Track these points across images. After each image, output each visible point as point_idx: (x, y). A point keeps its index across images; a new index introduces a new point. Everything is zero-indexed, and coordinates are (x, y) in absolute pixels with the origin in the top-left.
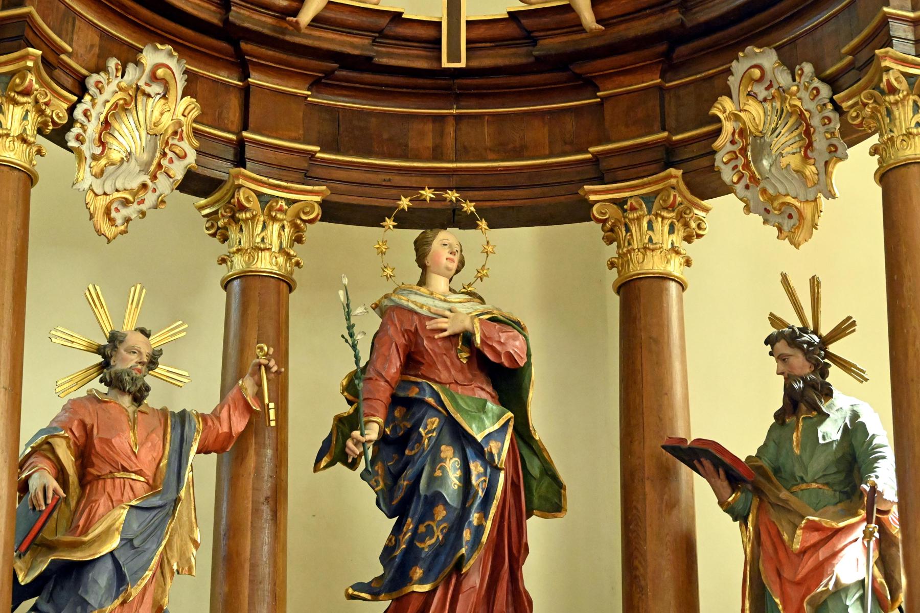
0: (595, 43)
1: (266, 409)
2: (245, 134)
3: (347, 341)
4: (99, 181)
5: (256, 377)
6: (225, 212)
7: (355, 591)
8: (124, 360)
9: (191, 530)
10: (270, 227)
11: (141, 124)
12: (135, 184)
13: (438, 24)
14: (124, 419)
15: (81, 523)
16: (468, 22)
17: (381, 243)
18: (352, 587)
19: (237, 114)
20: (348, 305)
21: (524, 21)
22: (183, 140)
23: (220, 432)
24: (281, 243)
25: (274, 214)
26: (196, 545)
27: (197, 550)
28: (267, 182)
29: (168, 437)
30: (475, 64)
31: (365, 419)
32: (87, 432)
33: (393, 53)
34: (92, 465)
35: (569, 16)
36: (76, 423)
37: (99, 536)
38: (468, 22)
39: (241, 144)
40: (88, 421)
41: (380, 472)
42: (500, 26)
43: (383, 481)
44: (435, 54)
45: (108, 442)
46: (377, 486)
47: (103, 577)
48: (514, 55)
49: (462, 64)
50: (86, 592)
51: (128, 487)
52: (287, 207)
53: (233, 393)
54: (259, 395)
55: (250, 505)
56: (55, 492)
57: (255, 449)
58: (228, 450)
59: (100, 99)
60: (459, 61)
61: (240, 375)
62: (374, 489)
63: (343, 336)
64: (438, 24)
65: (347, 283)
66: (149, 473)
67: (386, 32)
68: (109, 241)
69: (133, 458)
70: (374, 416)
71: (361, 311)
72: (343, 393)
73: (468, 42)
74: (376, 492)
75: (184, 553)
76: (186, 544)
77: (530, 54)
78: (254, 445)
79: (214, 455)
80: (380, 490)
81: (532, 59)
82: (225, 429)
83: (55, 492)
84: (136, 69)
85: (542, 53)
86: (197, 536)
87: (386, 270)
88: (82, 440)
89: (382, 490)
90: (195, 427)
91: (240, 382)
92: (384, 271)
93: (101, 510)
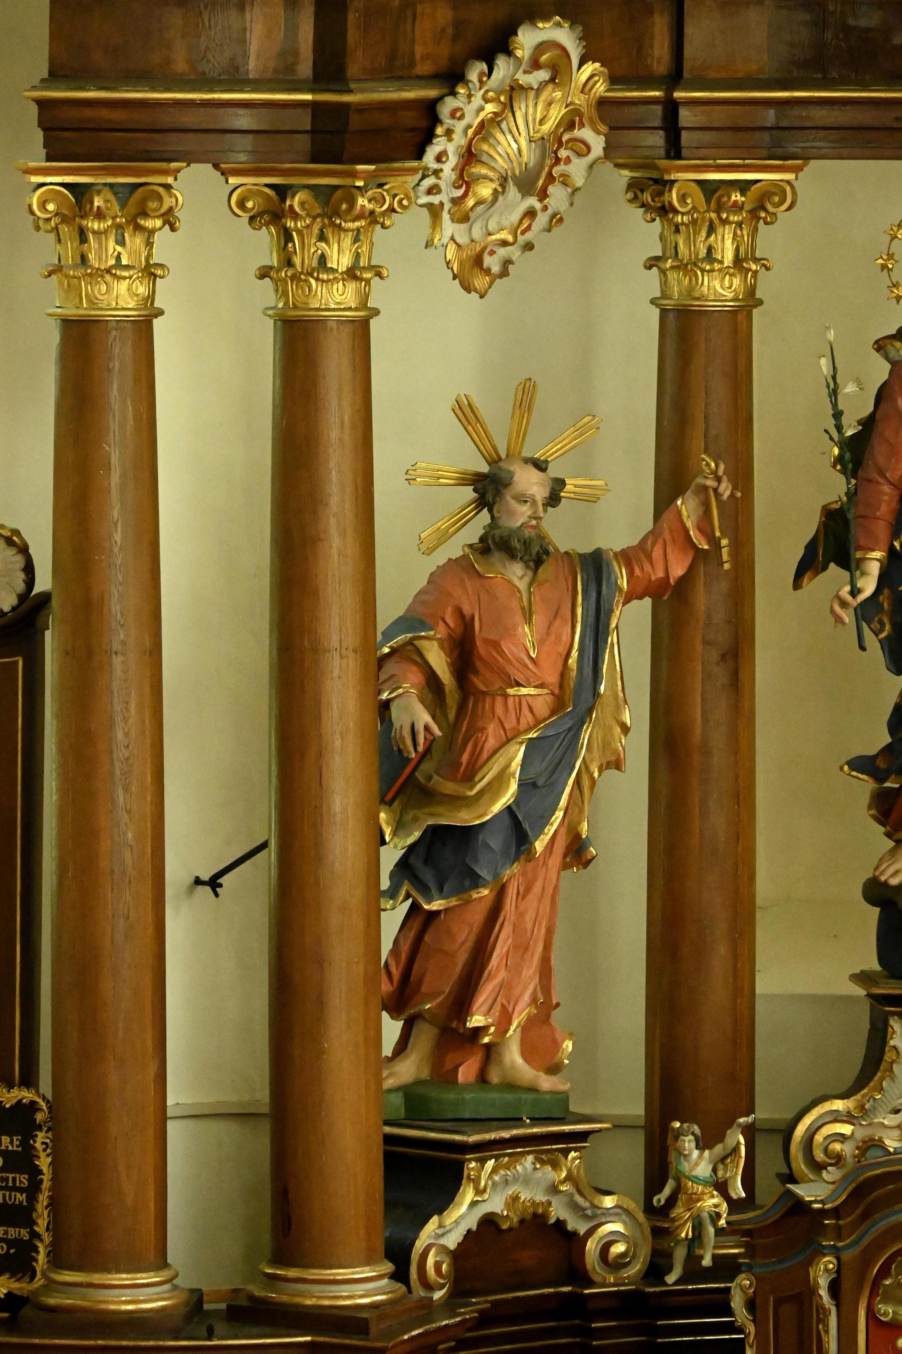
1: (715, 543)
2: (677, 95)
3: (831, 438)
4: (464, 226)
5: (702, 497)
6: (653, 200)
7: (853, 770)
8: (511, 513)
9: (618, 710)
10: (720, 230)
11: (521, 130)
12: (515, 217)
14: (515, 604)
15: (465, 758)
17: (885, 257)
18: (847, 763)
19: (666, 45)
20: (834, 378)
22: (584, 127)
23: (653, 579)
24: (737, 250)
25: (724, 216)
26: (625, 729)
27: (625, 736)
28: (714, 164)
29: (579, 611)
31: (859, 555)
32: (467, 624)
34: (476, 672)
36: (449, 610)
37: (489, 784)
39: (671, 108)
40: (467, 610)
41: (886, 605)
43: (890, 621)
45: (496, 645)
46: (882, 630)
47: (495, 841)
50: (476, 860)
51: (525, 710)
52: (743, 199)
53: (668, 515)
54: (705, 527)
55: (699, 668)
56: (427, 728)
57: (705, 583)
58: (665, 598)
59: (459, 126)
61: (679, 491)
62: (877, 635)
63: (826, 431)
65: (832, 339)
66: (552, 678)
68: (482, 297)
69: (530, 665)
70: (873, 550)
71: (853, 390)
72: (834, 467)
74: (880, 641)
75: (609, 744)
76: (611, 728)
78: (702, 577)
79: (648, 601)
80: (885, 638)
82: (660, 574)
83: (427, 728)
84: (508, 63)
86: (627, 718)
87: (895, 291)
88: (459, 631)
89: (888, 638)
90: (617, 582)
91: (679, 503)
92: (892, 292)
93: (491, 743)
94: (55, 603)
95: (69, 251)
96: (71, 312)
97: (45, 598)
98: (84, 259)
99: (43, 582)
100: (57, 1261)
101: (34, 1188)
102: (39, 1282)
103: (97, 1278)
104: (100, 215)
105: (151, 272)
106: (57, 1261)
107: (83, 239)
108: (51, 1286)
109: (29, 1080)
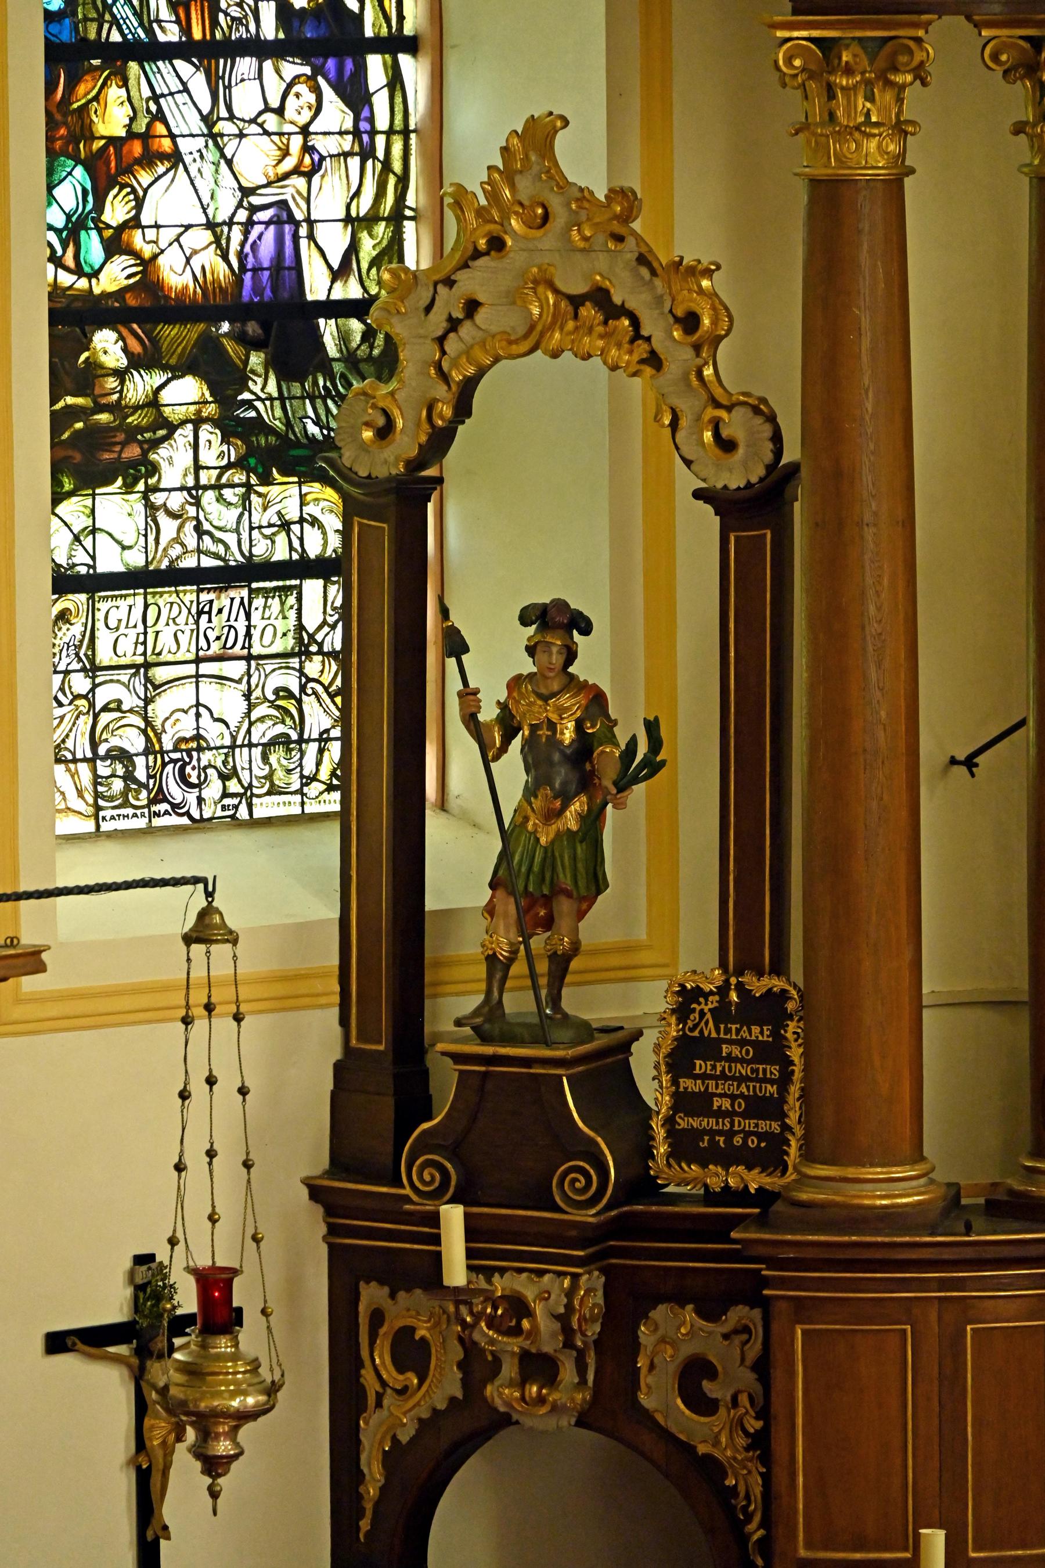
94: (804, 473)
95: (817, 108)
96: (820, 172)
97: (794, 469)
98: (832, 116)
99: (791, 453)
100: (809, 1155)
101: (785, 1080)
102: (791, 1176)
103: (851, 1172)
104: (848, 71)
105: (901, 129)
106: (809, 1155)
107: (831, 96)
108: (804, 1180)
109: (779, 968)
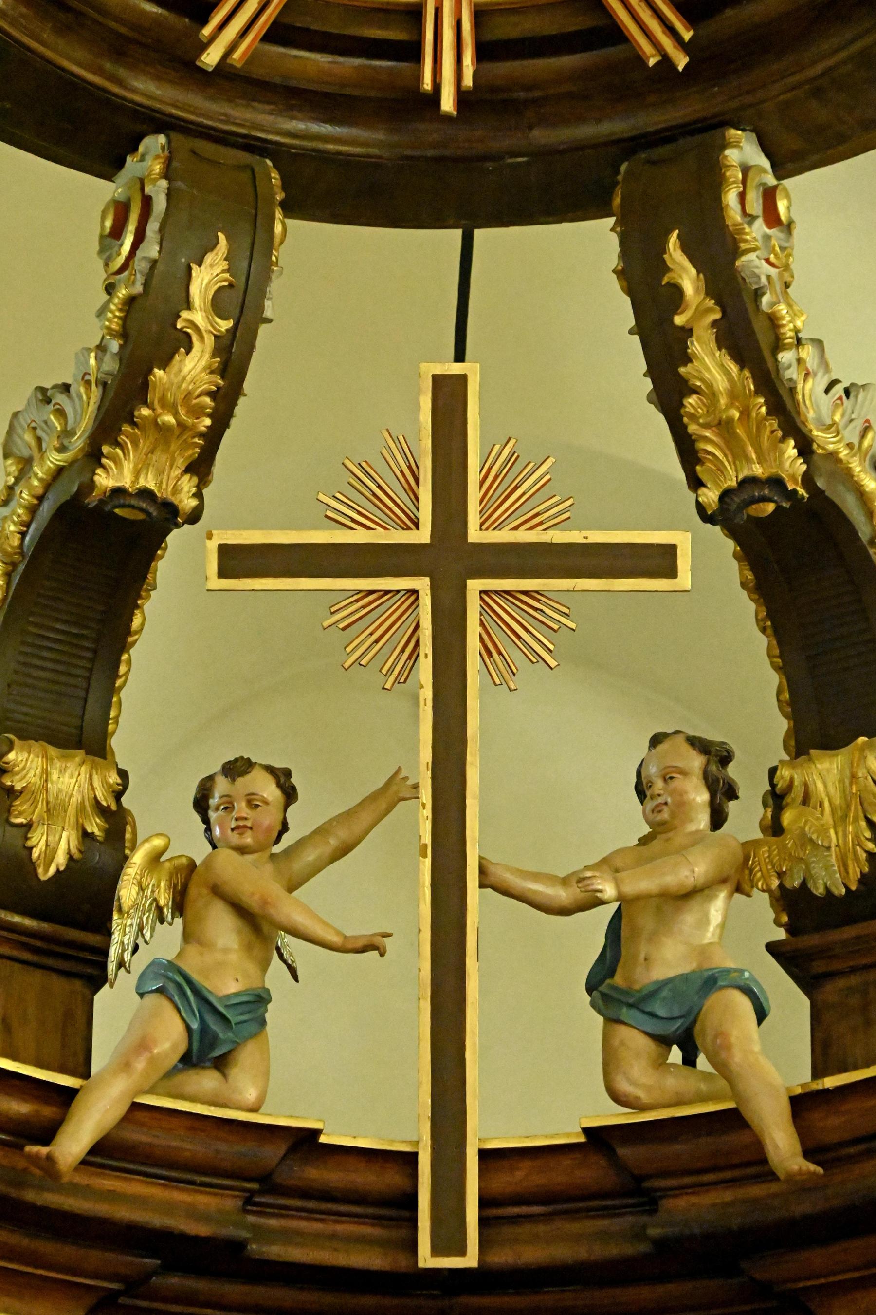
0: (803, 1207)
13: (410, 1159)
16: (484, 1154)
21: (623, 1152)
30: (503, 1257)
33: (299, 1233)
35: (736, 1139)
38: (484, 1154)
42: (566, 1161)
44: (400, 1233)
48: (604, 1236)
49: (470, 1260)
60: (462, 1251)
64: (410, 1159)
67: (279, 1179)
73: (484, 1203)
77: (639, 1235)
81: (643, 1248)
85: (668, 1231)
